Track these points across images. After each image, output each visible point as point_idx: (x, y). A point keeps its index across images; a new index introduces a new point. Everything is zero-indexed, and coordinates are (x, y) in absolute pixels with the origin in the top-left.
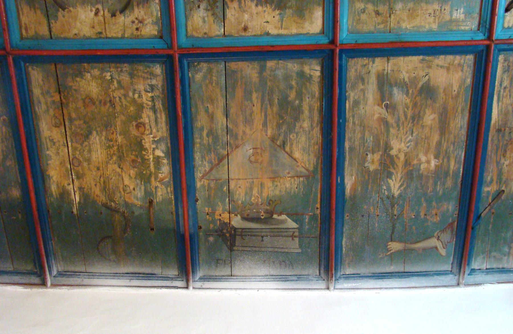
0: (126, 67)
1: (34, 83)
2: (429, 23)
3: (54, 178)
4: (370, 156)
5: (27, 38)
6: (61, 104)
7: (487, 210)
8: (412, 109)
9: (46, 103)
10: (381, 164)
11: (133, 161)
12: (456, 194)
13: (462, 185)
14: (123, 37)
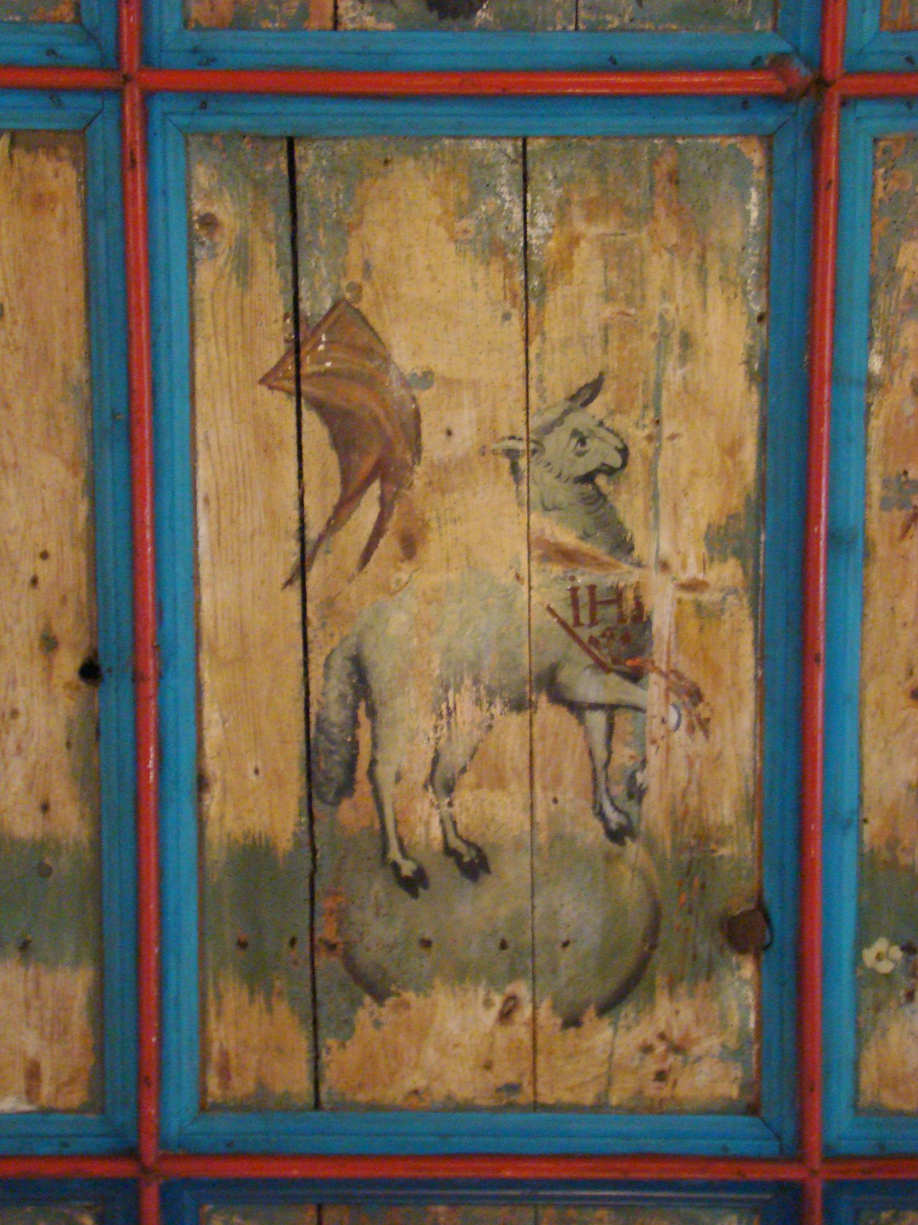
14: (600, 1107)
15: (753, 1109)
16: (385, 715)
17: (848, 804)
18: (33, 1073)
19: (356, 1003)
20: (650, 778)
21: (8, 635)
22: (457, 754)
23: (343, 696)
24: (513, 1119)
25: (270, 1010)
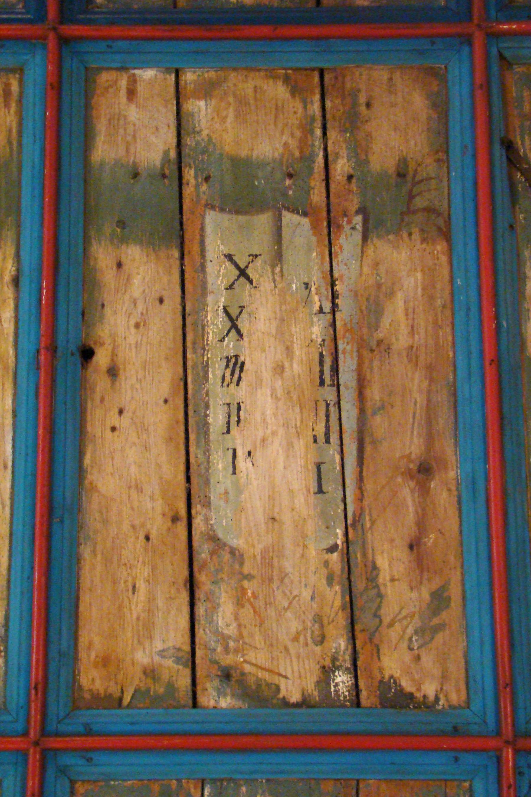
18: (131, 93)
21: (139, 377)
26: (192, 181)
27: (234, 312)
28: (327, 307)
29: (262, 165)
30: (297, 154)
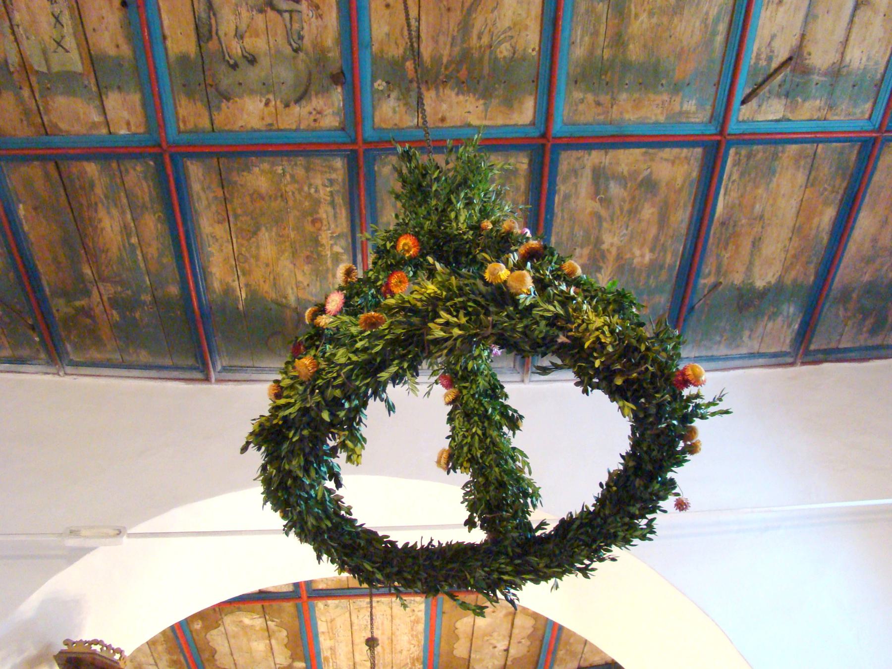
0: (301, 160)
1: (193, 178)
2: (656, 115)
3: (218, 274)
4: (578, 250)
5: (186, 132)
6: (225, 199)
7: (701, 302)
8: (630, 203)
9: (207, 199)
10: (589, 259)
11: (307, 257)
12: (669, 287)
13: (677, 277)
15: (343, 129)
16: (219, 16)
17: (367, 38)
18: (128, 124)
19: (221, 102)
20: (305, 33)
22: (243, 27)
23: (205, 10)
24: (271, 134)
25: (195, 104)
26: (92, 85)
27: (58, 25)
28: (16, 28)
29: (62, 94)
30: (49, 99)
